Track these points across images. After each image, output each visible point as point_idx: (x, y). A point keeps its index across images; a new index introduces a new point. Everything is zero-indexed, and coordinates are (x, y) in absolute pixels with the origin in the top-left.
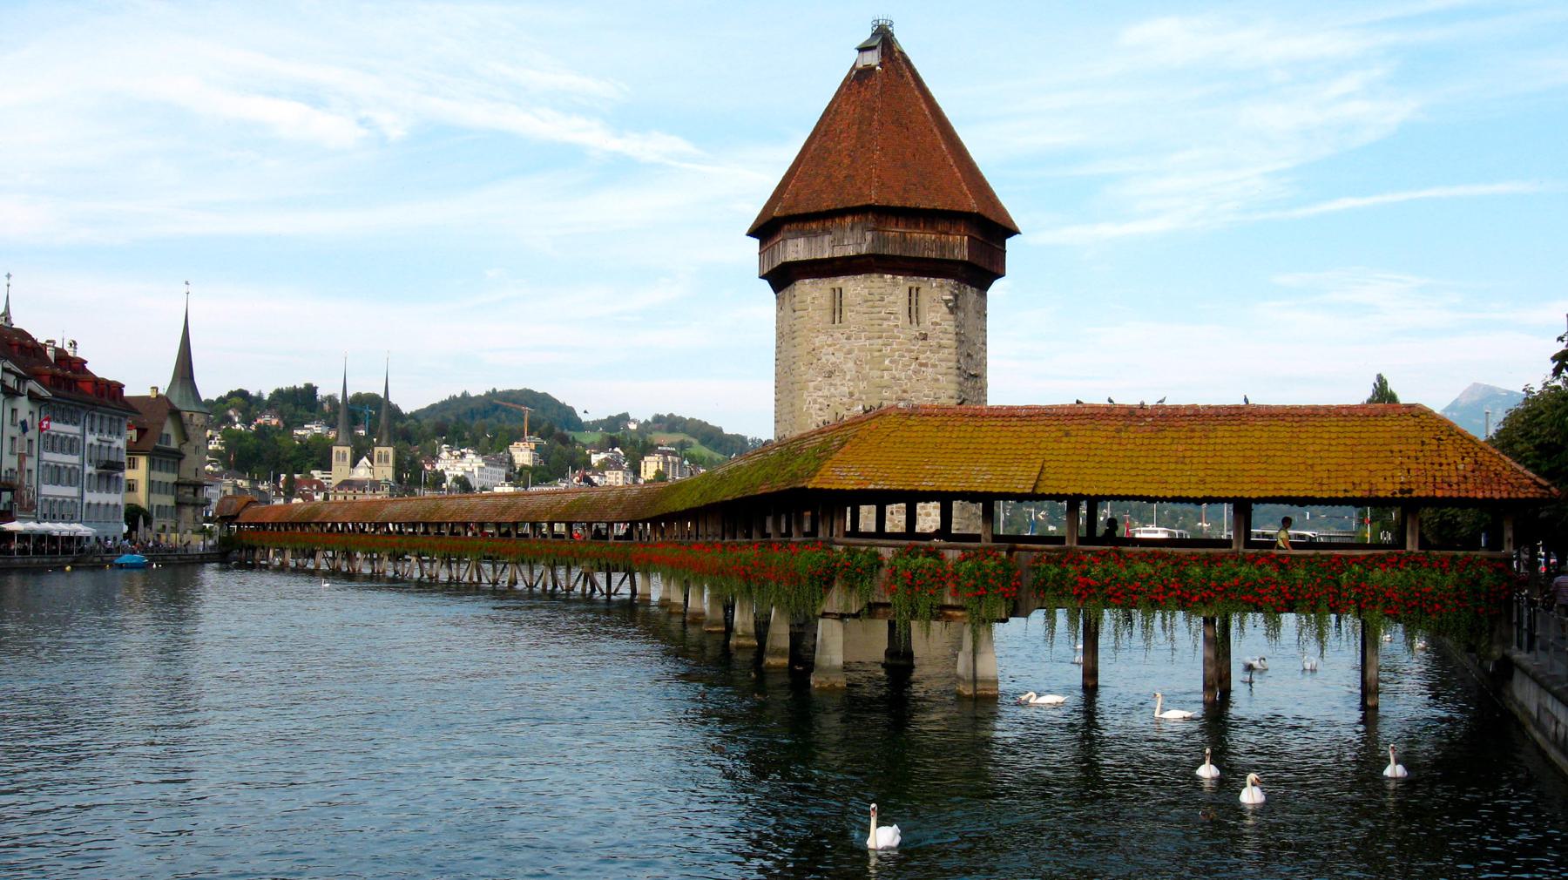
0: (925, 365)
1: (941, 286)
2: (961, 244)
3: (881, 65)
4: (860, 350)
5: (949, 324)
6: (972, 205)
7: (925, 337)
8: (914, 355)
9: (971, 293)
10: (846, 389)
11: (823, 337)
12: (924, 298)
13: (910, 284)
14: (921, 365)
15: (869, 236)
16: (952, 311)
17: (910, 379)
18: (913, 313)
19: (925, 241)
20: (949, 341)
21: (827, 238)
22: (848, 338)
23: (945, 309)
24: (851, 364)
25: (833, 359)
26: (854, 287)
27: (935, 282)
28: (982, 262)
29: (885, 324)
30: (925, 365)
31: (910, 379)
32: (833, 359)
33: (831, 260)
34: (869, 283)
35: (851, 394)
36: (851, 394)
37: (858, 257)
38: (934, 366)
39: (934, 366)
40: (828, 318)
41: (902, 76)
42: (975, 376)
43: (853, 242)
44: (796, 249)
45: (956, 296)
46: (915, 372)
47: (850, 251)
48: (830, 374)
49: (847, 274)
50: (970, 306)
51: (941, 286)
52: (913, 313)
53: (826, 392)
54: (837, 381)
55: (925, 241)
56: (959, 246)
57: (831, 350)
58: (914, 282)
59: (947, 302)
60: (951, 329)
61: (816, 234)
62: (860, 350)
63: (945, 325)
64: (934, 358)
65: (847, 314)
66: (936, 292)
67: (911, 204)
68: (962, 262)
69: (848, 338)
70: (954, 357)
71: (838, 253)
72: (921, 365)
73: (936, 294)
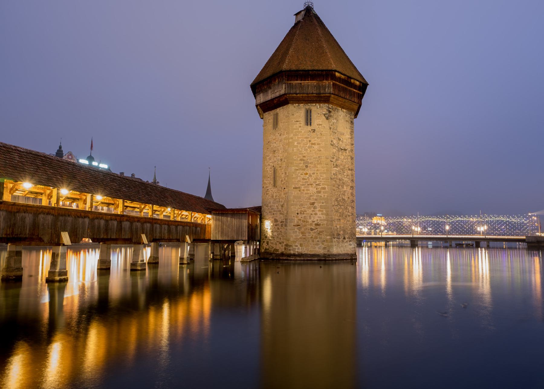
0: (314, 144)
3: (303, 19)
4: (285, 139)
8: (309, 139)
10: (280, 158)
12: (314, 115)
13: (307, 107)
14: (312, 144)
16: (327, 118)
17: (306, 150)
18: (308, 121)
21: (270, 91)
24: (282, 146)
26: (281, 112)
30: (314, 144)
31: (306, 150)
33: (272, 100)
35: (281, 160)
36: (281, 160)
38: (318, 144)
44: (262, 98)
46: (309, 147)
47: (277, 94)
49: (280, 106)
52: (308, 121)
57: (275, 141)
58: (308, 106)
64: (318, 141)
73: (319, 111)
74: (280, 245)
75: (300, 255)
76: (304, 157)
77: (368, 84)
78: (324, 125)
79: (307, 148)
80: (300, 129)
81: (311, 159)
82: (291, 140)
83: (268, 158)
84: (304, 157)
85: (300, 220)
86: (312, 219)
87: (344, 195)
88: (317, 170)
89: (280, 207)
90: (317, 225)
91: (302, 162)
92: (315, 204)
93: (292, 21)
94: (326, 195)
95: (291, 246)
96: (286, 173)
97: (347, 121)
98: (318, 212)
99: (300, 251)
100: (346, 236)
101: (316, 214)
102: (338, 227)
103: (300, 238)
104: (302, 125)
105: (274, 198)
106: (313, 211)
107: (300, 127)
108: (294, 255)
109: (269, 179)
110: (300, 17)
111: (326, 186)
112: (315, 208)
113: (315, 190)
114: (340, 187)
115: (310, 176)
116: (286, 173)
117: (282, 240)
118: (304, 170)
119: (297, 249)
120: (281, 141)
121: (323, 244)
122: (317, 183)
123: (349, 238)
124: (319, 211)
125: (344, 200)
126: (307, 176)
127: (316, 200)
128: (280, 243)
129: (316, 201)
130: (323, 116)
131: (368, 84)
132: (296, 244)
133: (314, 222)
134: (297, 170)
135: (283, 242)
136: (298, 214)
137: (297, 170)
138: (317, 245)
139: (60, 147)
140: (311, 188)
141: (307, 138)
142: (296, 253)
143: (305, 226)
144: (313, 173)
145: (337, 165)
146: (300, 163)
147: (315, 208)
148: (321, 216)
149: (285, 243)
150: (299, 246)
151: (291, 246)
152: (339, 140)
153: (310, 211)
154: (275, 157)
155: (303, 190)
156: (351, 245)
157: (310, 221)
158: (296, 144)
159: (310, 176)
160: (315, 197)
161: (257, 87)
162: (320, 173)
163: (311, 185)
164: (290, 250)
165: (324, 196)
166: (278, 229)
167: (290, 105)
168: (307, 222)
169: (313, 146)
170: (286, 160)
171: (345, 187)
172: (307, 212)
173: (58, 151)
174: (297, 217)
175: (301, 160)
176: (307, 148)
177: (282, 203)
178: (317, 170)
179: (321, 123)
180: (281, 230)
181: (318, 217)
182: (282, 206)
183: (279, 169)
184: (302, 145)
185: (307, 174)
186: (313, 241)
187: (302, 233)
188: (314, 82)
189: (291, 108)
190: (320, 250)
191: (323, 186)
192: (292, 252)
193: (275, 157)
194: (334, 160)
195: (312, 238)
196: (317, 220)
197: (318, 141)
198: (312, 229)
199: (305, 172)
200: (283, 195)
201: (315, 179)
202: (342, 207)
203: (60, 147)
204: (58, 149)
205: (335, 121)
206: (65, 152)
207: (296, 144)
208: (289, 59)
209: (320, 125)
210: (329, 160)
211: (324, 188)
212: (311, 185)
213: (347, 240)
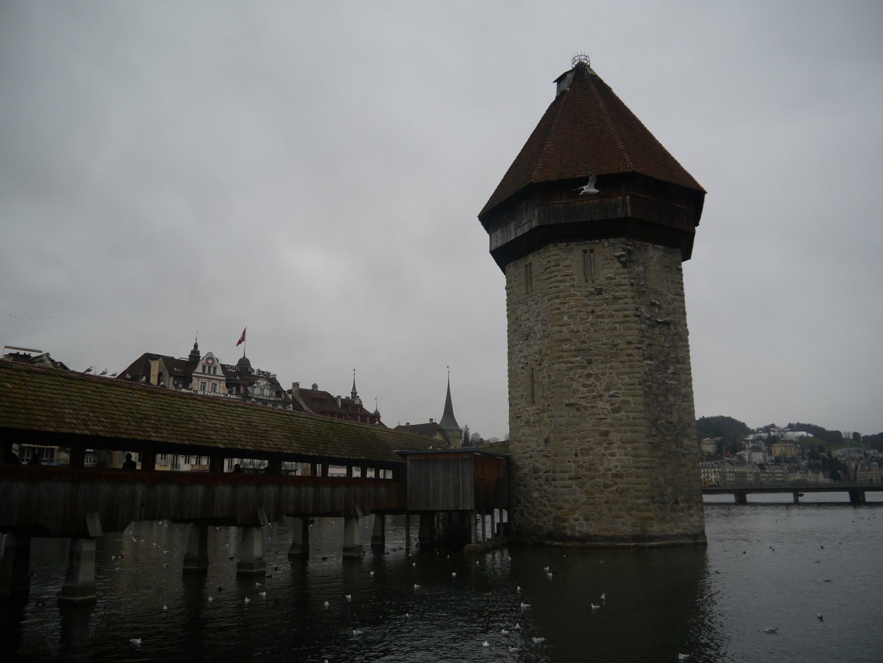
1: (613, 245)
3: (570, 87)
8: (590, 309)
9: (654, 254)
10: (537, 348)
11: (522, 307)
14: (598, 317)
16: (624, 265)
17: (588, 331)
21: (512, 224)
23: (619, 265)
24: (539, 325)
25: (529, 324)
30: (602, 316)
37: (532, 231)
38: (611, 316)
39: (611, 316)
40: (524, 291)
42: (667, 324)
45: (630, 252)
47: (526, 229)
48: (527, 337)
53: (525, 353)
54: (532, 342)
59: (618, 257)
69: (537, 304)
71: (519, 234)
72: (598, 317)
74: (545, 519)
75: (585, 538)
76: (584, 342)
77: (705, 192)
80: (572, 290)
84: (584, 342)
85: (581, 467)
86: (606, 464)
87: (671, 413)
88: (611, 367)
89: (542, 447)
90: (615, 476)
91: (581, 353)
92: (613, 436)
93: (550, 94)
94: (632, 415)
95: (566, 520)
96: (549, 376)
97: (666, 267)
98: (616, 450)
99: (585, 529)
100: (681, 498)
101: (613, 455)
102: (661, 479)
103: (584, 504)
105: (531, 424)
106: (606, 448)
107: (573, 286)
108: (573, 538)
109: (520, 389)
110: (565, 86)
111: (630, 398)
112: (611, 443)
113: (608, 406)
114: (661, 399)
115: (598, 379)
116: (549, 376)
117: (549, 509)
118: (584, 367)
119: (579, 525)
121: (631, 515)
122: (612, 393)
123: (687, 502)
124: (618, 448)
125: (671, 423)
126: (592, 380)
127: (611, 425)
128: (546, 515)
129: (611, 429)
131: (705, 192)
132: (576, 516)
133: (610, 470)
134: (571, 369)
135: (550, 513)
136: (576, 455)
137: (571, 369)
138: (618, 517)
139: (196, 346)
140: (600, 404)
141: (586, 305)
142: (577, 534)
143: (593, 478)
144: (604, 374)
145: (651, 354)
147: (611, 443)
148: (624, 458)
149: (554, 515)
150: (581, 518)
151: (566, 520)
152: (653, 304)
153: (600, 450)
155: (585, 408)
156: (691, 515)
157: (601, 468)
158: (565, 318)
159: (598, 379)
160: (609, 421)
161: (491, 217)
162: (618, 374)
163: (601, 396)
164: (564, 528)
165: (628, 418)
166: (541, 485)
168: (596, 470)
169: (600, 320)
171: (671, 399)
172: (596, 451)
173: (193, 352)
174: (575, 462)
177: (545, 437)
178: (611, 367)
179: (611, 275)
180: (545, 487)
181: (618, 460)
182: (546, 441)
183: (538, 368)
185: (589, 376)
186: (610, 509)
187: (587, 493)
189: (553, 253)
190: (626, 528)
191: (624, 398)
192: (568, 532)
194: (644, 346)
195: (607, 502)
196: (616, 467)
198: (606, 486)
199: (586, 372)
200: (546, 419)
201: (607, 385)
202: (668, 438)
203: (196, 346)
204: (193, 348)
205: (641, 268)
206: (203, 354)
207: (565, 318)
211: (627, 402)
212: (601, 396)
213: (681, 505)
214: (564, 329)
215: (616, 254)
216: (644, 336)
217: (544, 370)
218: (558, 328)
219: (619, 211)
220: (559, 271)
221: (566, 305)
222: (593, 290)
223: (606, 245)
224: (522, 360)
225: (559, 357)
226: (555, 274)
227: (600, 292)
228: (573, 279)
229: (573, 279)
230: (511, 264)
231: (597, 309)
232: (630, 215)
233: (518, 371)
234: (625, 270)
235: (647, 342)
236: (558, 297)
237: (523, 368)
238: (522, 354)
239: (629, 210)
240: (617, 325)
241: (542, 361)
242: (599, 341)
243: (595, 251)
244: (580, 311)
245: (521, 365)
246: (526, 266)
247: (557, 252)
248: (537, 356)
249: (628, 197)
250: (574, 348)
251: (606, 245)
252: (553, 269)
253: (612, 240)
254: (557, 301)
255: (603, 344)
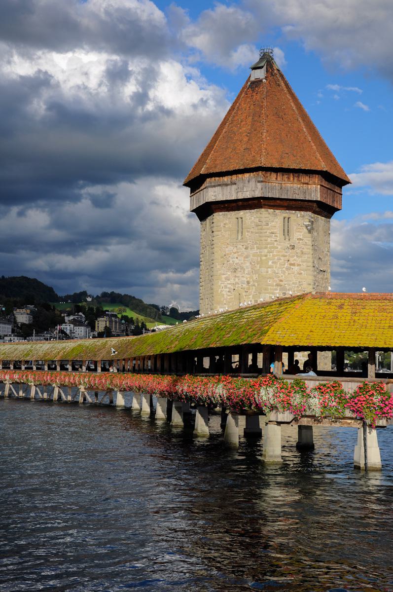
0: (293, 265)
1: (303, 216)
2: (316, 190)
5: (308, 240)
6: (323, 166)
7: (293, 247)
8: (287, 258)
11: (231, 248)
14: (291, 264)
15: (259, 185)
16: (310, 232)
18: (287, 232)
19: (293, 188)
20: (308, 250)
21: (234, 187)
22: (246, 248)
24: (248, 264)
25: (237, 261)
27: (299, 213)
28: (329, 202)
29: (269, 240)
30: (293, 265)
31: (284, 272)
32: (237, 261)
34: (259, 215)
35: (248, 283)
38: (299, 265)
39: (299, 265)
41: (279, 85)
43: (249, 187)
46: (287, 269)
48: (235, 270)
50: (320, 229)
51: (303, 216)
52: (287, 232)
53: (232, 281)
55: (293, 188)
56: (314, 191)
57: (236, 255)
59: (307, 227)
60: (310, 243)
61: (227, 185)
62: (254, 256)
63: (306, 240)
64: (299, 261)
65: (246, 234)
66: (300, 219)
67: (285, 166)
68: (316, 202)
69: (246, 248)
70: (311, 260)
71: (240, 197)
72: (291, 264)
78: (306, 240)
79: (284, 269)
80: (275, 243)
81: (289, 285)
82: (264, 258)
83: (223, 276)
91: (279, 288)
104: (278, 239)
107: (276, 241)
120: (247, 257)
130: (304, 228)
141: (285, 256)
146: (276, 290)
154: (236, 276)
158: (270, 263)
167: (263, 210)
169: (292, 267)
170: (256, 284)
175: (277, 285)
176: (284, 269)
179: (301, 237)
183: (244, 294)
184: (278, 265)
188: (296, 186)
189: (264, 214)
193: (236, 276)
197: (299, 261)
207: (270, 263)
208: (266, 149)
209: (301, 239)
210: (311, 287)
214: (269, 269)
215: (305, 223)
216: (316, 280)
217: (251, 296)
218: (266, 269)
219: (312, 195)
220: (268, 229)
221: (271, 254)
222: (289, 246)
223: (299, 215)
224: (229, 286)
225: (266, 289)
226: (265, 231)
227: (293, 247)
228: (276, 236)
229: (276, 236)
230: (221, 213)
231: (291, 259)
232: (319, 199)
233: (225, 293)
234: (310, 235)
235: (316, 284)
236: (266, 248)
237: (229, 292)
238: (229, 282)
239: (319, 196)
240: (302, 272)
241: (249, 289)
242: (291, 281)
243: (291, 220)
244: (280, 259)
245: (228, 290)
246: (238, 218)
247: (267, 215)
248: (244, 286)
249: (319, 186)
250: (275, 284)
251: (299, 215)
252: (264, 227)
253: (302, 213)
254: (266, 250)
255: (293, 283)
